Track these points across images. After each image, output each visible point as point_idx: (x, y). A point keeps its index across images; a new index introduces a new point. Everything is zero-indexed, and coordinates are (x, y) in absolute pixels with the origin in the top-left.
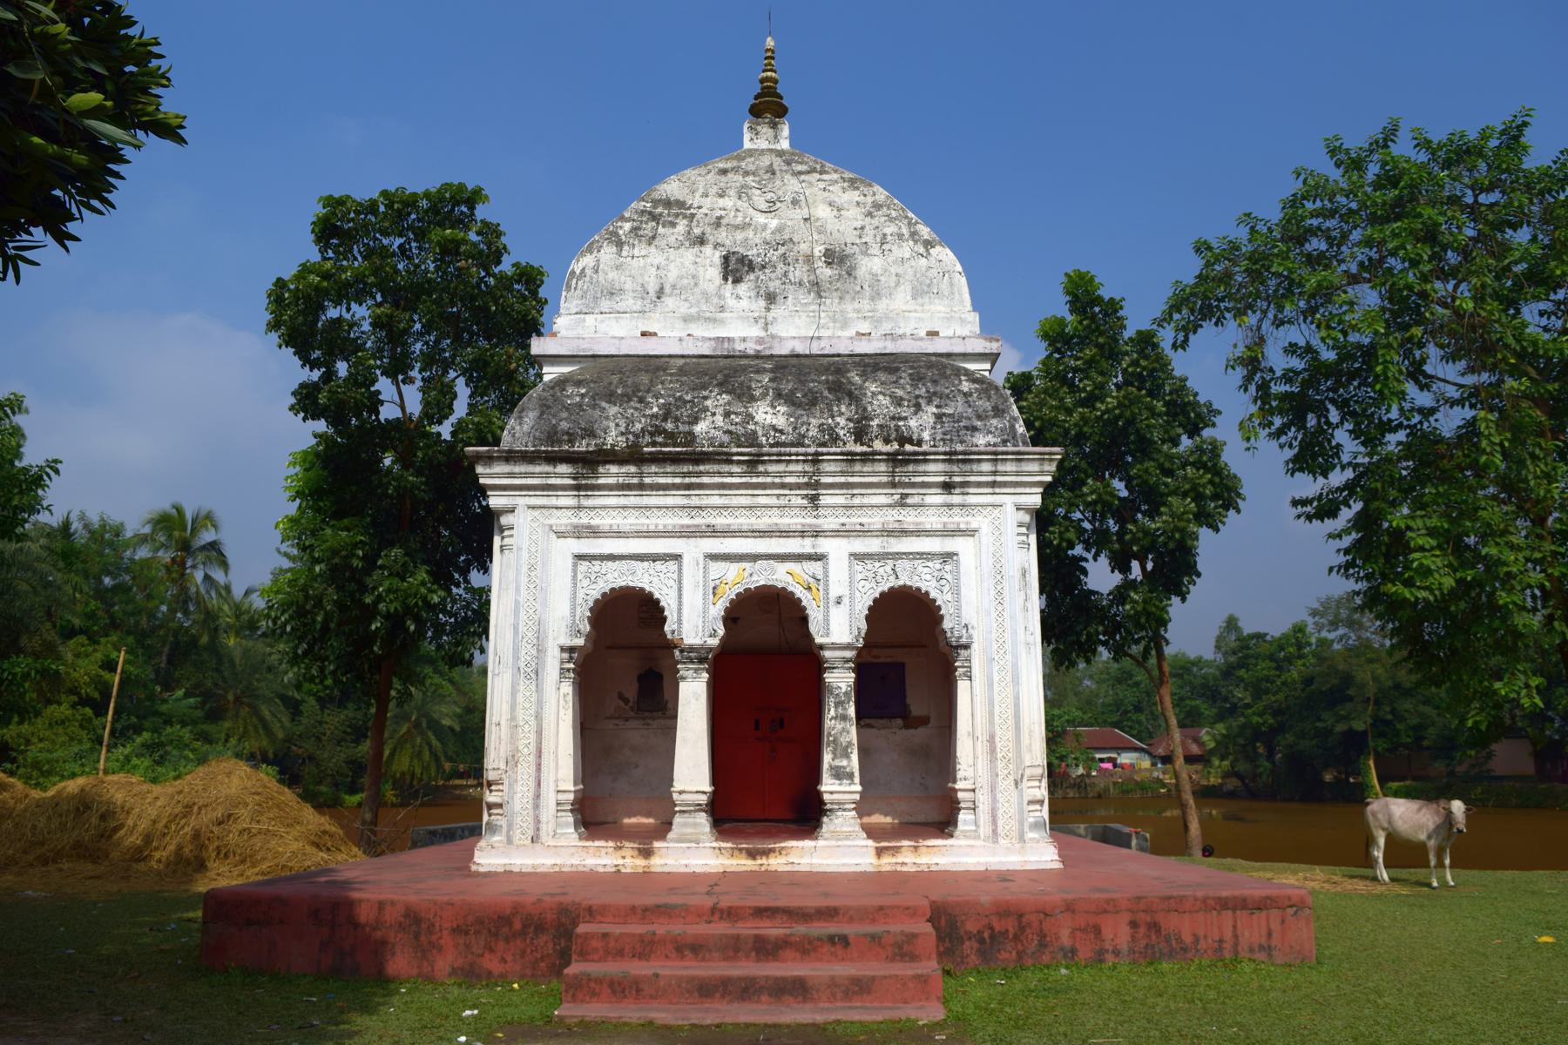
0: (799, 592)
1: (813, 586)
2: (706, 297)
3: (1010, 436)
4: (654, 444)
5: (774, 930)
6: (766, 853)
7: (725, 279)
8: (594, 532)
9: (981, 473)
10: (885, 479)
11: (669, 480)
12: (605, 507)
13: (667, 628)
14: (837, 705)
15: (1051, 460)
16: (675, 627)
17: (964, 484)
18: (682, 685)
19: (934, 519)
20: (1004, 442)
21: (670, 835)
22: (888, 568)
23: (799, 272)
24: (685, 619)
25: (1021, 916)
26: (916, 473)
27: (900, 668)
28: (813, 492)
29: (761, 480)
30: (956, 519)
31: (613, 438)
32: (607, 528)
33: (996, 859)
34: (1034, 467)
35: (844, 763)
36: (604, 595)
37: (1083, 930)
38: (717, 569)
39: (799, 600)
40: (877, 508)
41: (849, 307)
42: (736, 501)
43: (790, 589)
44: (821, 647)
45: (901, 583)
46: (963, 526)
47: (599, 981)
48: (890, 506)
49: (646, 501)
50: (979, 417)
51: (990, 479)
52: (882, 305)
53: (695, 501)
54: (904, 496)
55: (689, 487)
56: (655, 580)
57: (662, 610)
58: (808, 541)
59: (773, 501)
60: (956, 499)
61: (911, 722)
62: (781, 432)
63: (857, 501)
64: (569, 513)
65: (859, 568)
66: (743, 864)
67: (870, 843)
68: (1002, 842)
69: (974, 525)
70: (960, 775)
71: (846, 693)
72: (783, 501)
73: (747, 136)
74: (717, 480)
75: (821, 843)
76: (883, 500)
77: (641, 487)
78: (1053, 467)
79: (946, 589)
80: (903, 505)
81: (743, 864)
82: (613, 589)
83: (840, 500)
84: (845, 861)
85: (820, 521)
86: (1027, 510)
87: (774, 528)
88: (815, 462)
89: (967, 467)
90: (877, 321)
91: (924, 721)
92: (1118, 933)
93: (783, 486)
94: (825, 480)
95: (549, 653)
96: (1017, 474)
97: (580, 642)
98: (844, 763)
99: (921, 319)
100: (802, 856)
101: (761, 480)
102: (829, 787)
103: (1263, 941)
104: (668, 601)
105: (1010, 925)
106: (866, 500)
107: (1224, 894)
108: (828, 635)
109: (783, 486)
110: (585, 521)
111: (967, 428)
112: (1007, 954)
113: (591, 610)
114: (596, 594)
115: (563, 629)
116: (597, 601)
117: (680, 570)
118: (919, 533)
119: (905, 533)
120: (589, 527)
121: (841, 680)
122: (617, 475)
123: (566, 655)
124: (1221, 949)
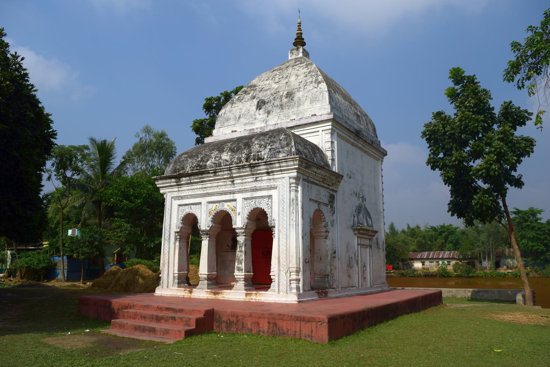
0: (230, 211)
2: (251, 116)
3: (290, 153)
4: (197, 170)
5: (160, 314)
6: (218, 293)
7: (257, 109)
9: (276, 168)
10: (250, 173)
11: (197, 181)
12: (184, 190)
14: (240, 247)
15: (296, 160)
17: (273, 172)
20: (288, 155)
21: (198, 287)
22: (253, 202)
23: (277, 103)
25: (237, 317)
26: (258, 170)
28: (232, 179)
29: (218, 177)
30: (272, 184)
31: (188, 170)
33: (277, 299)
34: (291, 163)
37: (254, 323)
40: (249, 182)
41: (291, 111)
42: (220, 184)
47: (117, 323)
50: (282, 148)
51: (279, 169)
52: (301, 108)
53: (204, 186)
54: (257, 178)
55: (202, 182)
58: (232, 195)
59: (222, 184)
60: (271, 177)
62: (227, 161)
63: (244, 181)
66: (212, 296)
67: (245, 292)
68: (281, 293)
70: (272, 270)
72: (225, 184)
73: (290, 55)
74: (208, 179)
75: (232, 291)
76: (251, 180)
77: (191, 183)
78: (297, 162)
80: (257, 181)
81: (212, 296)
83: (240, 181)
84: (238, 297)
86: (294, 178)
88: (230, 170)
89: (271, 166)
90: (298, 114)
92: (264, 326)
93: (225, 179)
94: (234, 175)
96: (287, 166)
98: (240, 266)
99: (311, 111)
100: (228, 295)
101: (218, 177)
102: (236, 273)
103: (310, 333)
104: (199, 217)
105: (234, 319)
106: (247, 180)
107: (298, 315)
109: (225, 179)
111: (277, 152)
112: (233, 329)
118: (261, 189)
122: (185, 180)
124: (295, 335)
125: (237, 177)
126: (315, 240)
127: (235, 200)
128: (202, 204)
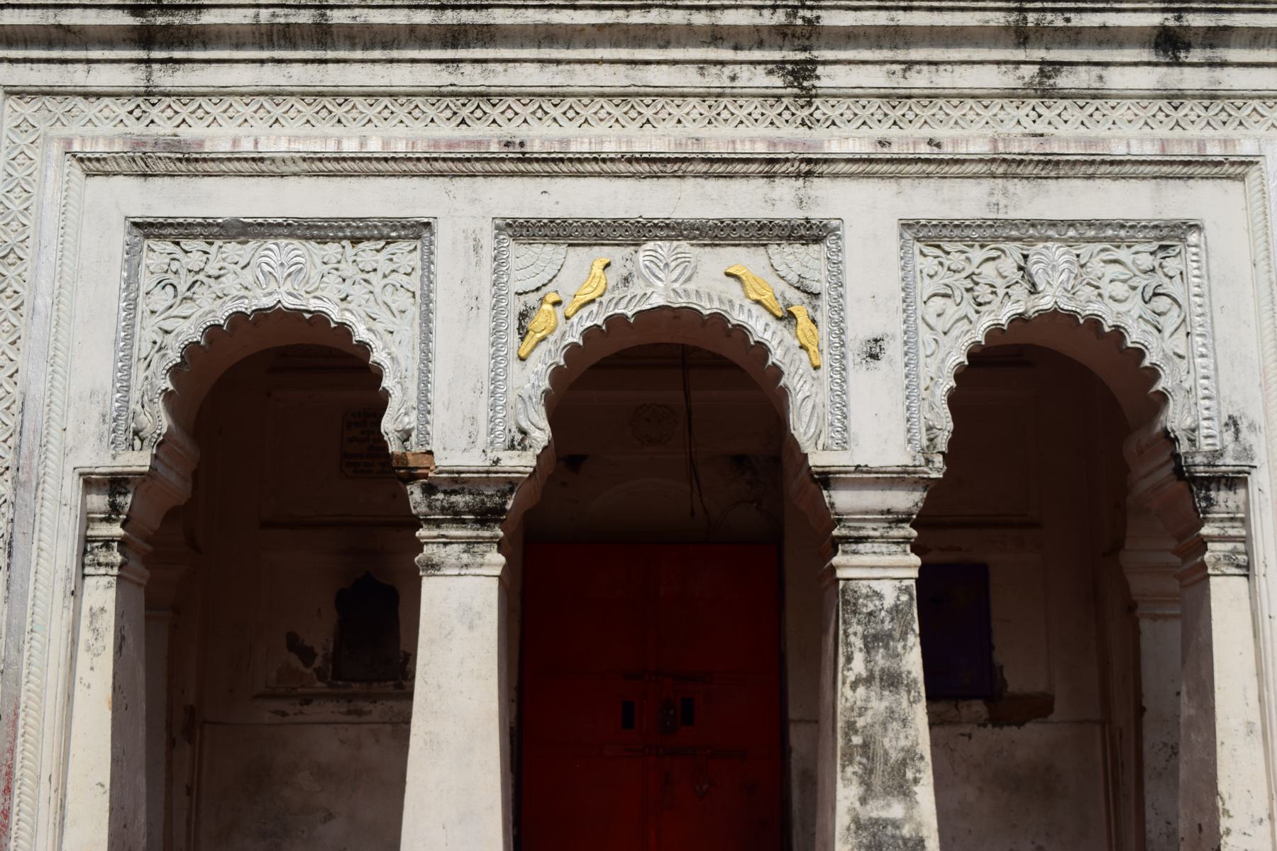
0: (761, 327)
1: (801, 312)
8: (191, 162)
12: (221, 93)
13: (389, 425)
14: (872, 642)
16: (411, 421)
17: (1216, 37)
18: (430, 586)
19: (1133, 131)
22: (1009, 265)
24: (438, 397)
27: (981, 572)
28: (797, 49)
30: (1193, 132)
32: (224, 147)
35: (896, 810)
36: (213, 331)
39: (762, 350)
40: (975, 102)
43: (736, 317)
44: (826, 479)
45: (1046, 303)
46: (1214, 150)
48: (1010, 95)
49: (333, 76)
53: (471, 77)
54: (1049, 68)
55: (456, 36)
56: (358, 292)
57: (375, 374)
59: (688, 78)
60: (1192, 79)
61: (1009, 710)
63: (920, 80)
64: (119, 108)
65: (929, 265)
69: (1246, 148)
71: (896, 611)
72: (715, 79)
76: (990, 78)
79: (1169, 323)
80: (1047, 94)
82: (237, 318)
83: (874, 78)
85: (819, 133)
87: (691, 149)
91: (1036, 708)
93: (716, 36)
95: (50, 489)
97: (139, 460)
98: (896, 810)
104: (392, 353)
106: (946, 79)
108: (844, 445)
109: (716, 36)
110: (164, 128)
113: (175, 372)
114: (191, 331)
115: (93, 426)
116: (191, 350)
117: (428, 263)
119: (1052, 166)
120: (172, 144)
121: (881, 574)
123: (99, 501)
125: (850, 37)
126: (1145, 625)
127: (811, 233)
128: (443, 236)
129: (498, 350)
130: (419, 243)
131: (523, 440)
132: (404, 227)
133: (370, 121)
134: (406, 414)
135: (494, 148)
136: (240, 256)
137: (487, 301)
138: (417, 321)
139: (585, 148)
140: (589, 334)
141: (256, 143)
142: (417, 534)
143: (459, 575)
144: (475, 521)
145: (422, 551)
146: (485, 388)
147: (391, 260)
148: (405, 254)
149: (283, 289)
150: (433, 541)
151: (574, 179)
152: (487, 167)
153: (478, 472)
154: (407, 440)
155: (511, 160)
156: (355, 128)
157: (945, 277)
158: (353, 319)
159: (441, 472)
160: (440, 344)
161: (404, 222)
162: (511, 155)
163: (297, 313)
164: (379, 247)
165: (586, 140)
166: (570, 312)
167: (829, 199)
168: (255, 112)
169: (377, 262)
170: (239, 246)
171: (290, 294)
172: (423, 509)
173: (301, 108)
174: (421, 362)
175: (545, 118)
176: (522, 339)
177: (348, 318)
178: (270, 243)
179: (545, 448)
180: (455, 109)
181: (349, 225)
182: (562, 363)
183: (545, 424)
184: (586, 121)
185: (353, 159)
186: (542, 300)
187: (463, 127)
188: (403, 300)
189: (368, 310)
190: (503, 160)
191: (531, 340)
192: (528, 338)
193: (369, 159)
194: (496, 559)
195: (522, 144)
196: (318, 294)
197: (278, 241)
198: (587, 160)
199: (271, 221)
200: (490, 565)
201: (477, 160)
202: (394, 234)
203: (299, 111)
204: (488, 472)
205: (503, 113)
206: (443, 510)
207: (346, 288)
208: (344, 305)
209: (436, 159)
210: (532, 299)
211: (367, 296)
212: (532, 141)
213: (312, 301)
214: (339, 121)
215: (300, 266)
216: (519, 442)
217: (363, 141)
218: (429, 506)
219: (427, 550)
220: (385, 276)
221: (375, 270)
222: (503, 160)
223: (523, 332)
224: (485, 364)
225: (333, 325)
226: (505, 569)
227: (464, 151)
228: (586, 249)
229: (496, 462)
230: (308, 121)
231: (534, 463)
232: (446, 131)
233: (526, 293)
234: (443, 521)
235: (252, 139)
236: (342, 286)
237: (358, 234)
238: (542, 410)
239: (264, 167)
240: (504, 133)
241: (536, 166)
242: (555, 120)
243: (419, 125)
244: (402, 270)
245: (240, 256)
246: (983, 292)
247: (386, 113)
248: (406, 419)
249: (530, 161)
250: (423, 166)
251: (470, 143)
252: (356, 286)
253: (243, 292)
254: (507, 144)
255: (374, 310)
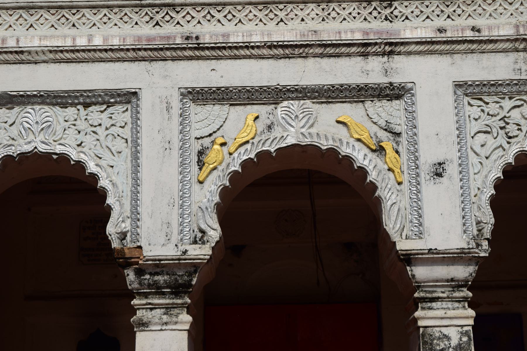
0: (361, 157)
1: (388, 146)
13: (111, 229)
16: (126, 226)
24: (144, 210)
38: (206, 117)
39: (363, 172)
43: (345, 150)
44: (409, 259)
56: (89, 140)
57: (103, 194)
65: (475, 112)
85: (398, 25)
87: (312, 38)
104: (113, 182)
108: (420, 235)
127: (394, 92)
128: (146, 101)
129: (184, 177)
130: (129, 106)
131: (202, 237)
132: (119, 95)
133: (94, 25)
134: (123, 221)
135: (179, 41)
136: (8, 117)
137: (176, 144)
138: (129, 158)
139: (240, 39)
140: (245, 164)
141: (18, 41)
142: (132, 303)
143: (161, 330)
144: (171, 293)
145: (136, 314)
146: (176, 202)
147: (111, 118)
148: (120, 114)
149: (38, 139)
150: (143, 307)
151: (233, 61)
152: (174, 54)
153: (172, 260)
154: (124, 239)
155: (190, 48)
156: (85, 30)
157: (485, 120)
158: (86, 158)
159: (147, 260)
160: (145, 174)
161: (119, 92)
162: (190, 46)
163: (48, 155)
164: (102, 109)
165: (240, 34)
166: (232, 149)
167: (405, 69)
168: (17, 20)
169: (101, 119)
170: (8, 111)
171: (43, 142)
172: (136, 285)
173: (47, 17)
174: (133, 186)
175: (212, 20)
176: (200, 169)
177: (83, 157)
178: (29, 109)
179: (217, 242)
180: (151, 15)
181: (82, 95)
182: (228, 184)
183: (217, 226)
184: (240, 21)
185: (83, 51)
186: (213, 142)
187: (157, 27)
188: (119, 145)
189: (96, 152)
190: (184, 49)
191: (206, 169)
192: (204, 168)
193: (95, 50)
194: (186, 318)
195: (197, 38)
196: (61, 142)
197: (34, 107)
198: (241, 47)
199: (29, 93)
200: (182, 323)
201: (167, 49)
202: (112, 100)
203: (47, 19)
204: (179, 259)
205: (184, 17)
206: (149, 286)
207: (81, 137)
208: (80, 149)
209: (139, 49)
210: (207, 142)
211: (95, 143)
212: (204, 35)
213: (58, 147)
214: (74, 25)
215: (49, 123)
216: (201, 238)
217: (90, 38)
218: (140, 284)
219: (139, 313)
220: (107, 129)
221: (100, 125)
222: (184, 49)
223: (201, 164)
224: (176, 186)
225: (72, 163)
226: (192, 325)
227: (158, 43)
228: (242, 107)
229: (185, 252)
230: (53, 26)
231: (210, 253)
232: (146, 30)
233: (202, 138)
234: (150, 293)
235: (15, 38)
236: (78, 136)
237: (88, 101)
238: (215, 216)
239: (23, 57)
240: (185, 31)
241: (207, 53)
242: (219, 21)
243: (128, 27)
244: (118, 125)
245: (8, 117)
246: (512, 129)
247: (105, 19)
248: (123, 225)
249: (203, 49)
250: (130, 54)
251: (162, 38)
252: (88, 136)
253: (11, 142)
254: (187, 38)
255: (100, 151)
